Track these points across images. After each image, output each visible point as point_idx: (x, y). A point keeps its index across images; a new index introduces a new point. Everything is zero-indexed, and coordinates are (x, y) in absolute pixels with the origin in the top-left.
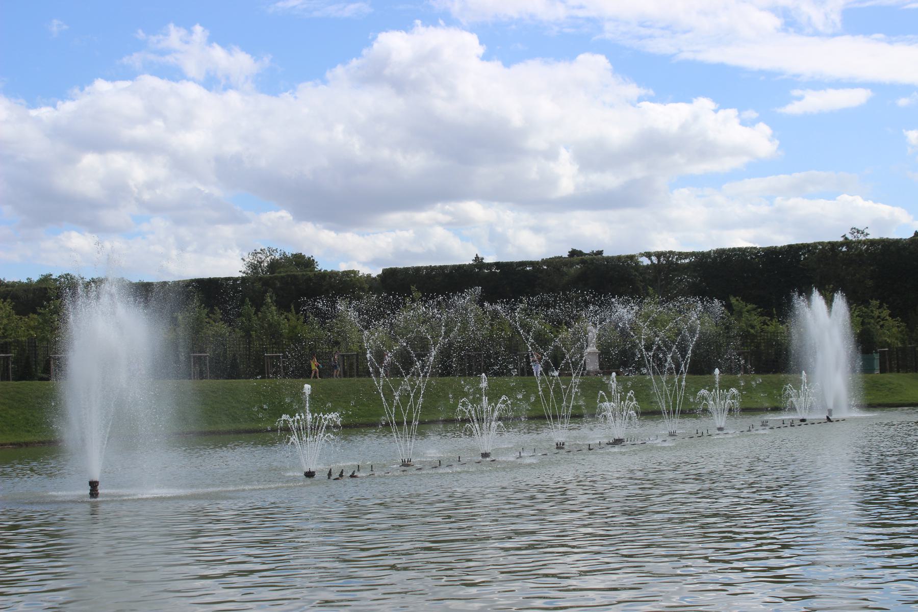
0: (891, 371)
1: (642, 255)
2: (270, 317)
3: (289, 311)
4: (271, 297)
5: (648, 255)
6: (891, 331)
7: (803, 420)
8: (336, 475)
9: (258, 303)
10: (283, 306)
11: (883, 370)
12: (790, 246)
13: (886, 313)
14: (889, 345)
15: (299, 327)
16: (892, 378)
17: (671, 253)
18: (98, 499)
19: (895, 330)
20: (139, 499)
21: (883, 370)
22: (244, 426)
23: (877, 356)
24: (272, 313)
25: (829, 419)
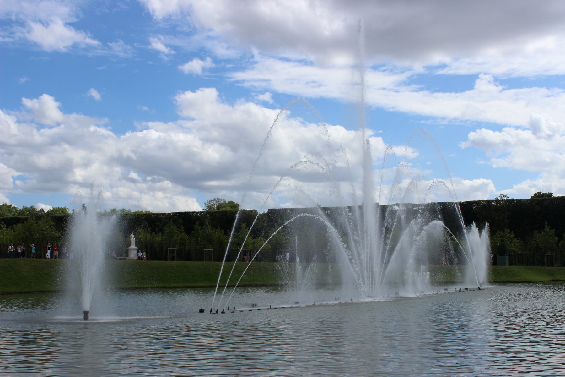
0: (515, 265)
1: (395, 205)
2: (207, 232)
3: (217, 228)
4: (208, 221)
5: (398, 205)
6: (515, 244)
7: (466, 289)
8: (214, 312)
9: (202, 225)
10: (214, 226)
11: (511, 264)
12: (468, 202)
13: (513, 236)
14: (514, 252)
15: (222, 237)
16: (515, 268)
17: (409, 204)
18: (87, 322)
19: (517, 244)
20: (99, 323)
21: (511, 264)
22: (182, 285)
23: (507, 257)
24: (209, 230)
25: (479, 289)
